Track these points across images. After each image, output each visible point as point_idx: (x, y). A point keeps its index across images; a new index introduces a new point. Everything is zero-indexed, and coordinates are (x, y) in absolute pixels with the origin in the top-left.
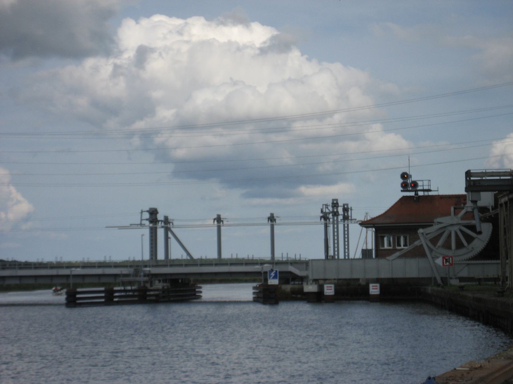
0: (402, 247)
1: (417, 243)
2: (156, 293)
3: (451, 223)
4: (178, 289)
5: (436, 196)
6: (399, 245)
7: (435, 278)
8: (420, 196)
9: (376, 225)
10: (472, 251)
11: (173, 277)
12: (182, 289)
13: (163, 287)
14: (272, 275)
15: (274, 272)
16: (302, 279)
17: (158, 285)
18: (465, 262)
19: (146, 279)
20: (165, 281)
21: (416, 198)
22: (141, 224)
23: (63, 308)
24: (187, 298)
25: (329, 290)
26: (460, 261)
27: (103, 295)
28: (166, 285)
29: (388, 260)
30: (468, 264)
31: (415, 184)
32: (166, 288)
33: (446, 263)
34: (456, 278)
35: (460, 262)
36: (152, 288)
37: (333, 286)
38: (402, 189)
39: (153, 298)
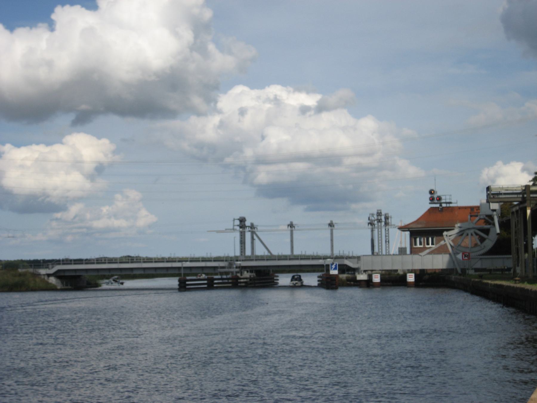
0: (430, 245)
1: (442, 243)
2: (245, 280)
3: (468, 227)
4: (261, 278)
5: (456, 207)
6: (428, 244)
7: (456, 269)
8: (443, 207)
9: (410, 229)
10: (483, 248)
11: (257, 269)
12: (264, 277)
13: (250, 276)
14: (333, 268)
15: (335, 264)
16: (355, 270)
17: (246, 274)
18: (479, 257)
19: (238, 270)
20: (251, 272)
21: (441, 208)
22: (233, 229)
23: (177, 291)
24: (268, 284)
25: (377, 279)
27: (206, 282)
28: (253, 275)
29: (421, 256)
30: (481, 259)
31: (439, 198)
32: (252, 277)
33: (465, 257)
34: (472, 269)
36: (242, 277)
37: (379, 275)
38: (430, 202)
39: (243, 284)
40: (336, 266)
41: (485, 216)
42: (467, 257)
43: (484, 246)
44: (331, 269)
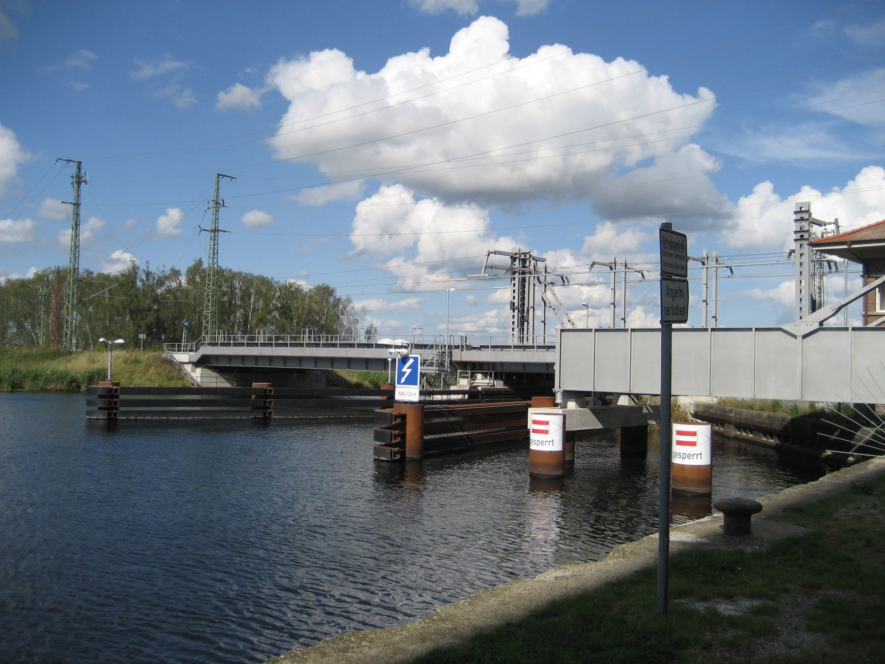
2: (460, 397)
14: (405, 373)
15: (411, 361)
29: (795, 337)
40: (414, 367)
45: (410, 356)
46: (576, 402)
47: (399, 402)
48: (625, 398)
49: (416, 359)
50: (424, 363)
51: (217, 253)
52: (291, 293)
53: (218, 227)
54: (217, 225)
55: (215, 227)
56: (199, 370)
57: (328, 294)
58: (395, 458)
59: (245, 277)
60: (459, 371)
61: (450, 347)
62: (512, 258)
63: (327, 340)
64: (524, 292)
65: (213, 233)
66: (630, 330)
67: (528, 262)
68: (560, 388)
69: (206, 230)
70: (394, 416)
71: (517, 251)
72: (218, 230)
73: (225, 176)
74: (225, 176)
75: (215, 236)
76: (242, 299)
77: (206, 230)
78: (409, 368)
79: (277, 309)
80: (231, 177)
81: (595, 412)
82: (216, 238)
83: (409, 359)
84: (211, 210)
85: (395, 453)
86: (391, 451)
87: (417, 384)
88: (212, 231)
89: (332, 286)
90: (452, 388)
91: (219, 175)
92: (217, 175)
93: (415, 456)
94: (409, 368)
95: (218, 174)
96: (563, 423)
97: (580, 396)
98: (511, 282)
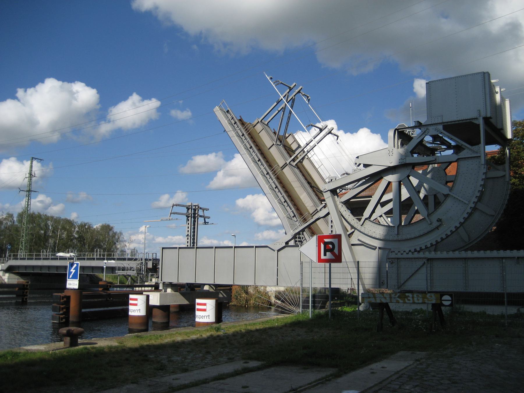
10: (437, 228)
14: (72, 272)
15: (75, 265)
18: (421, 255)
26: (410, 251)
29: (274, 250)
30: (429, 260)
33: (325, 255)
35: (410, 255)
40: (76, 269)
41: (441, 127)
42: (332, 251)
43: (439, 220)
44: (69, 278)
45: (75, 262)
46: (171, 288)
47: (68, 289)
48: (207, 287)
49: (77, 264)
50: (131, 269)
51: (30, 204)
52: (85, 228)
53: (31, 189)
54: (30, 188)
55: (29, 189)
56: (7, 275)
57: (108, 230)
58: (62, 321)
59: (56, 219)
60: (150, 274)
61: (146, 260)
62: (187, 208)
63: (90, 256)
64: (194, 228)
65: (28, 193)
66: (178, 248)
67: (197, 211)
68: (162, 281)
69: (23, 191)
70: (62, 297)
71: (190, 204)
72: (31, 191)
73: (37, 159)
74: (37, 159)
75: (29, 194)
76: (53, 232)
77: (23, 191)
78: (74, 269)
79: (76, 238)
80: (40, 160)
81: (183, 294)
82: (30, 195)
83: (74, 264)
84: (28, 179)
85: (62, 319)
86: (59, 317)
87: (77, 279)
88: (27, 191)
89: (111, 225)
90: (146, 284)
91: (33, 158)
92: (31, 158)
93: (75, 320)
94: (74, 269)
95: (32, 158)
96: (147, 300)
97: (176, 287)
98: (187, 222)
